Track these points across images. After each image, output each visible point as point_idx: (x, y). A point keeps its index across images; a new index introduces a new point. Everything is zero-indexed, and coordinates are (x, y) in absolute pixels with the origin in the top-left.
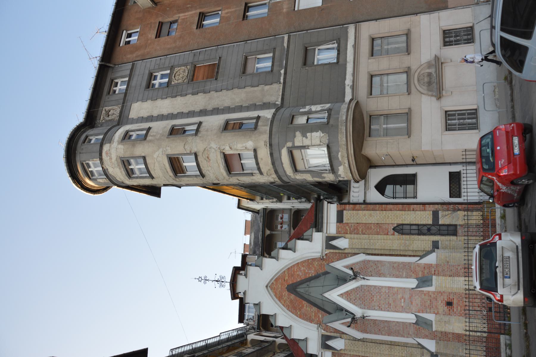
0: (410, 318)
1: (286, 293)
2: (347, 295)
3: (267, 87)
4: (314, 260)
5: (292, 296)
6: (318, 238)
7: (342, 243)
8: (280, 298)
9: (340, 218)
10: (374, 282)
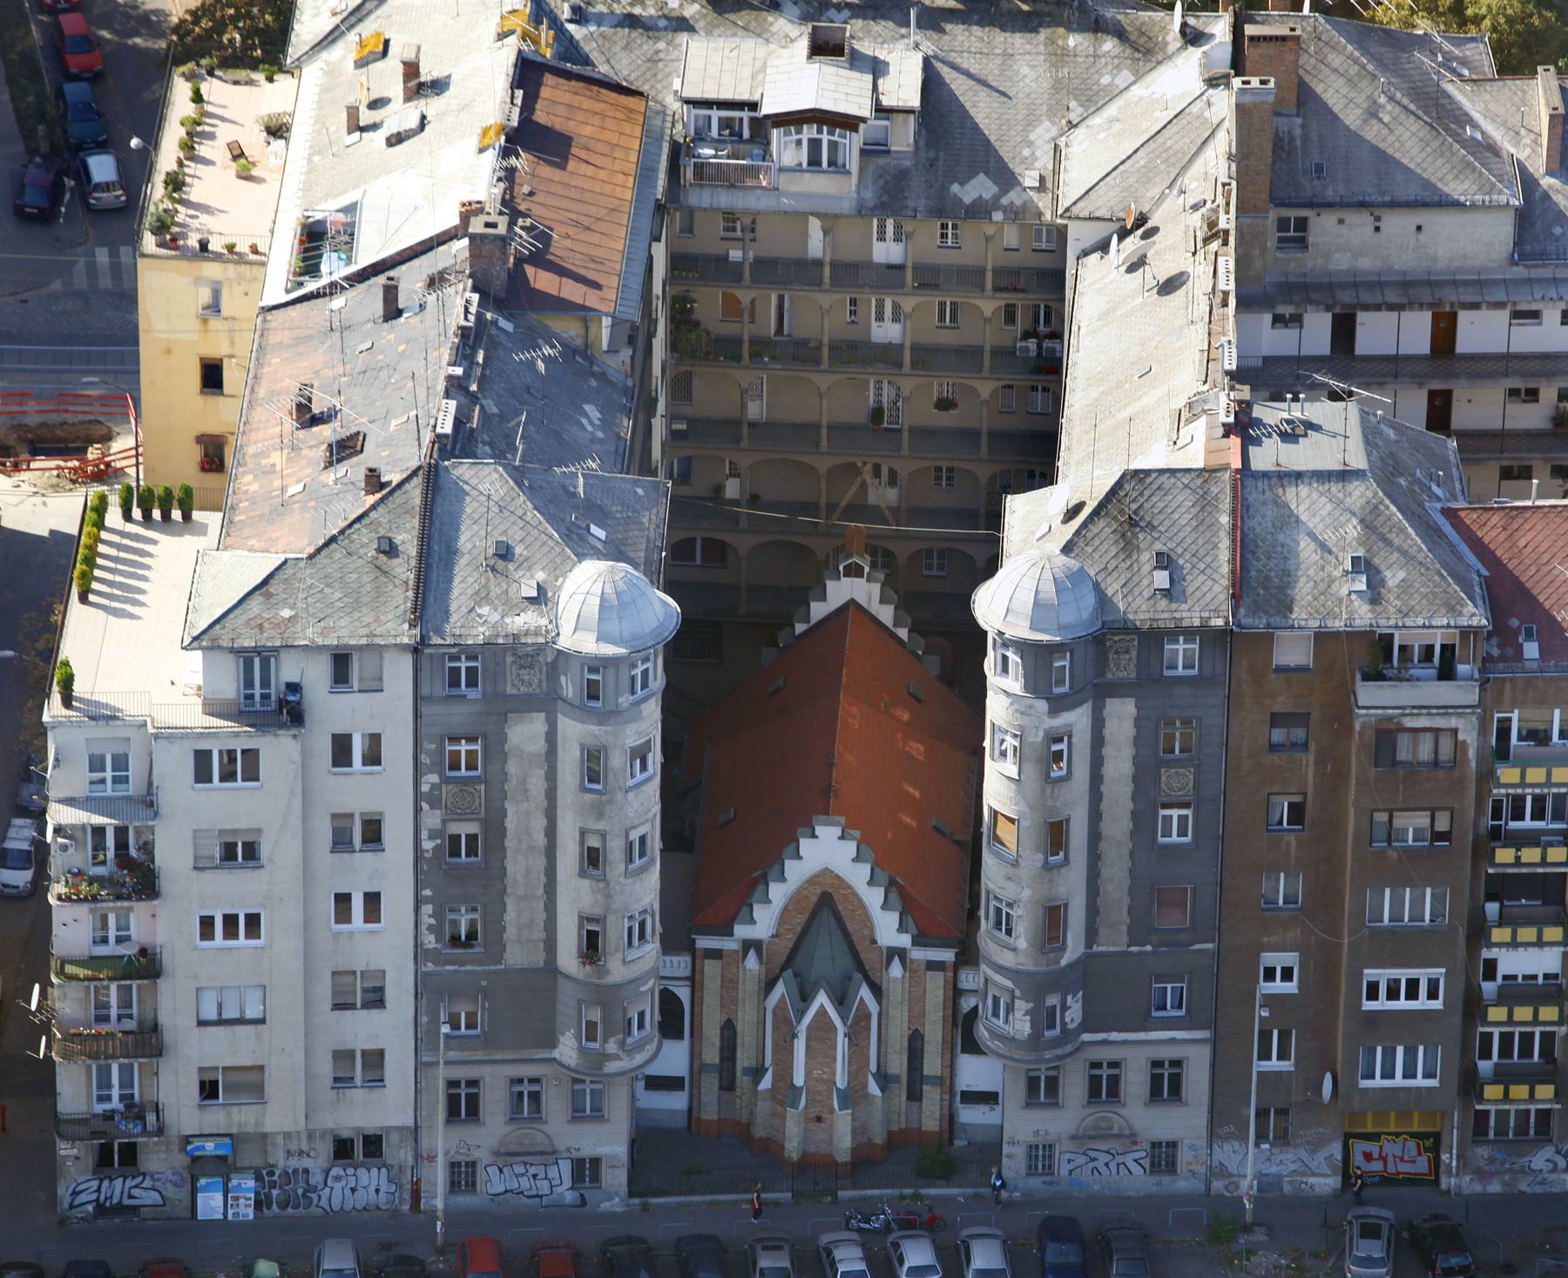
0: (799, 1080)
1: (819, 891)
2: (822, 1011)
3: (1124, 929)
4: (872, 929)
5: (814, 899)
6: (905, 940)
7: (896, 970)
8: (812, 881)
9: (933, 966)
10: (841, 1042)
